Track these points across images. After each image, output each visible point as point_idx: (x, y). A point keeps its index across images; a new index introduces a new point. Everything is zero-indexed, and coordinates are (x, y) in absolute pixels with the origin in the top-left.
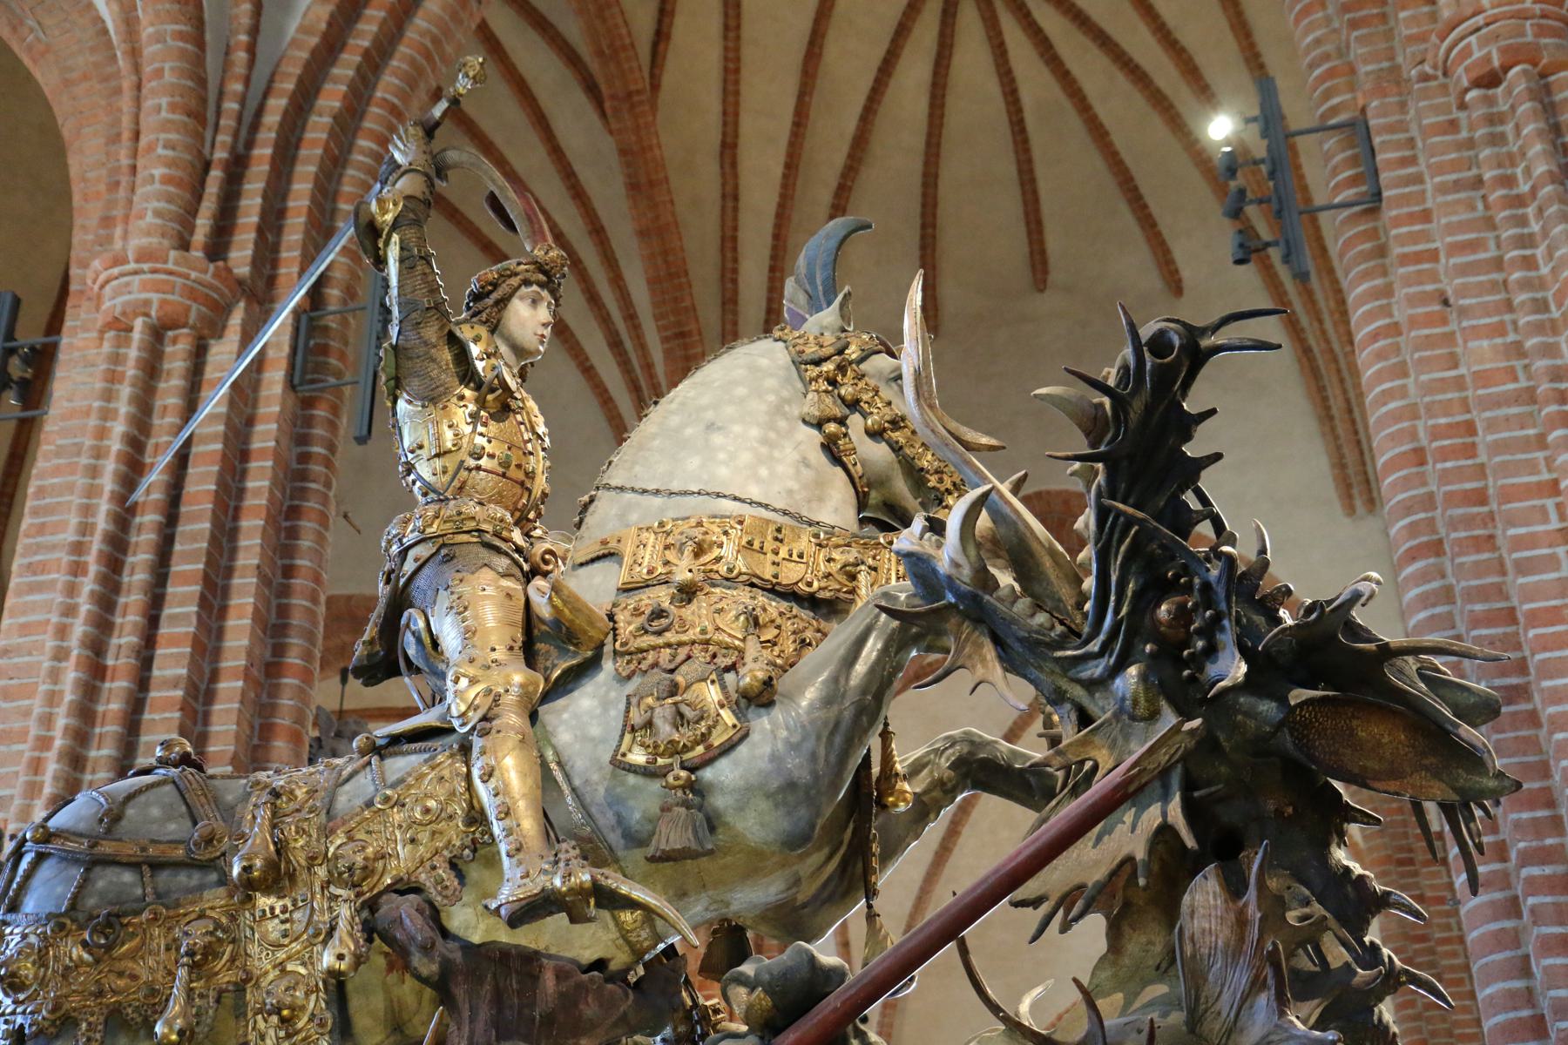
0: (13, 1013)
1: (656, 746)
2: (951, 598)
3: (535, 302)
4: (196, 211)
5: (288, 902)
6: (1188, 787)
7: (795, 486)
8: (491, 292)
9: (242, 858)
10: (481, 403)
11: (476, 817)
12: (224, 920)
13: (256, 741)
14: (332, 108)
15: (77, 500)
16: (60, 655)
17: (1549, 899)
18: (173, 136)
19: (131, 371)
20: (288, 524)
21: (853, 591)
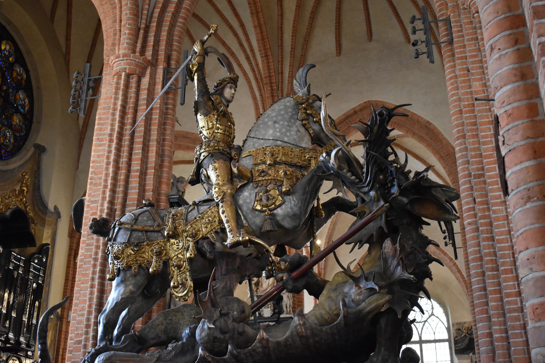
0: (117, 264)
2: (332, 172)
3: (231, 88)
4: (137, 42)
5: (178, 241)
6: (387, 217)
7: (296, 137)
9: (167, 231)
10: (218, 116)
11: (221, 222)
12: (163, 245)
13: (158, 185)
14: (172, 11)
15: (109, 122)
16: (108, 164)
17: (485, 228)
18: (131, 22)
21: (310, 164)
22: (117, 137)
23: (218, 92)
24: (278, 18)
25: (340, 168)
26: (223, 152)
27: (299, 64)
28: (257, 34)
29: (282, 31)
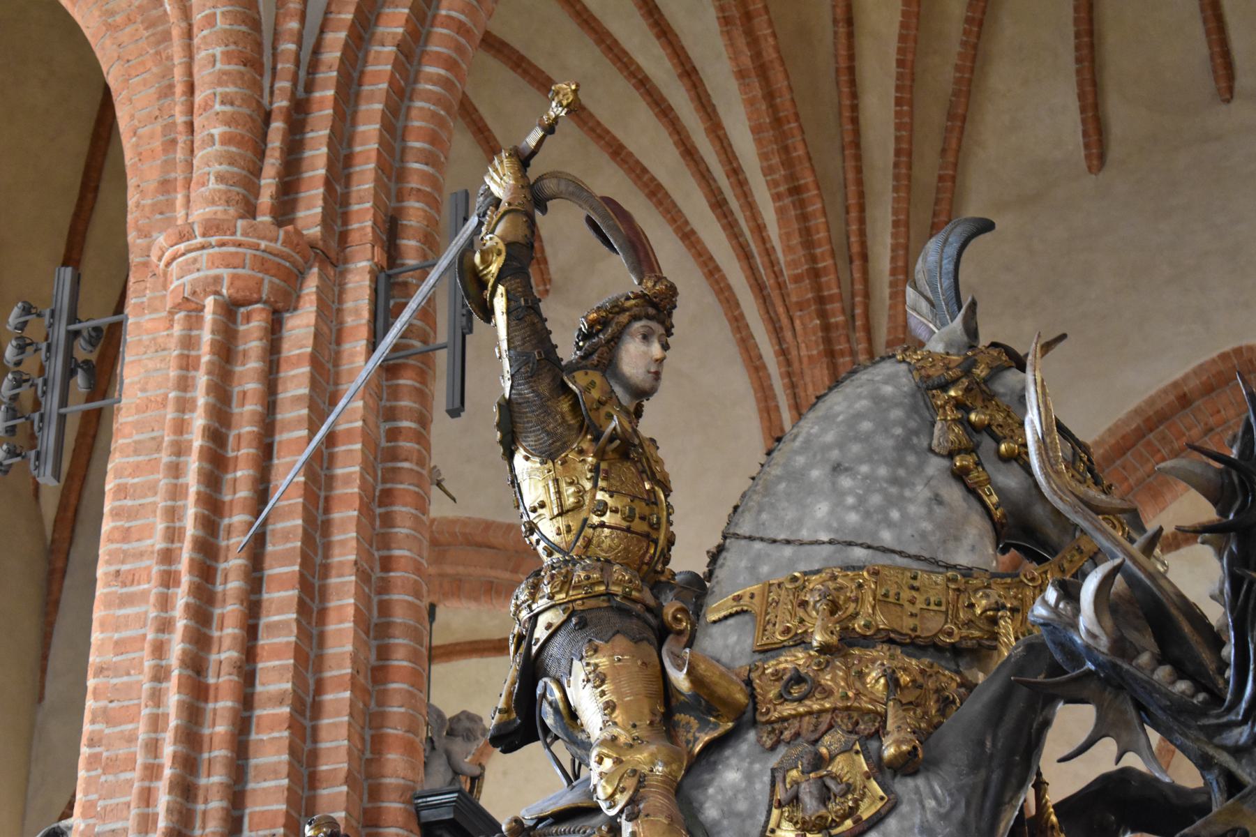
1: (804, 823)
2: (1090, 666)
3: (646, 338)
4: (261, 169)
7: (927, 526)
8: (599, 331)
10: (600, 455)
13: (368, 755)
14: (395, 34)
15: (161, 501)
16: (160, 675)
18: (231, 89)
19: (205, 355)
20: (382, 510)
21: (995, 636)
22: (192, 560)
23: (595, 357)
24: (835, 33)
25: (1121, 647)
26: (628, 604)
27: (935, 215)
28: (750, 103)
29: (853, 83)
